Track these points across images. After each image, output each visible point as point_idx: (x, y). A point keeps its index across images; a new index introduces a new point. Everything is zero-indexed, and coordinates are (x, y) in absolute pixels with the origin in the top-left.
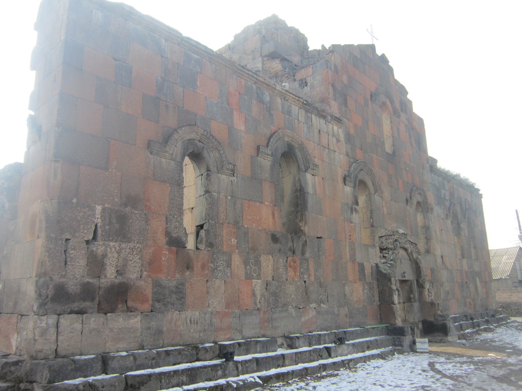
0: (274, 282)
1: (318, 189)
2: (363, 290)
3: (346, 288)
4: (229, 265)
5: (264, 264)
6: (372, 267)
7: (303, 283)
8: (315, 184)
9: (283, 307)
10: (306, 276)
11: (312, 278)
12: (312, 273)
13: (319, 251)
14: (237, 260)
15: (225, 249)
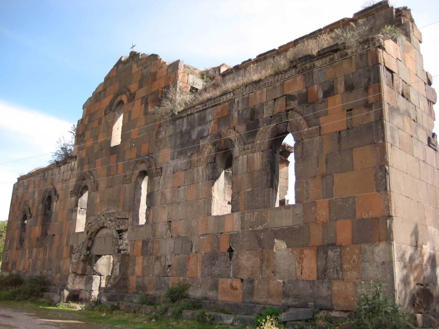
1: (57, 208)
11: (47, 257)
12: (47, 255)
14: (27, 251)
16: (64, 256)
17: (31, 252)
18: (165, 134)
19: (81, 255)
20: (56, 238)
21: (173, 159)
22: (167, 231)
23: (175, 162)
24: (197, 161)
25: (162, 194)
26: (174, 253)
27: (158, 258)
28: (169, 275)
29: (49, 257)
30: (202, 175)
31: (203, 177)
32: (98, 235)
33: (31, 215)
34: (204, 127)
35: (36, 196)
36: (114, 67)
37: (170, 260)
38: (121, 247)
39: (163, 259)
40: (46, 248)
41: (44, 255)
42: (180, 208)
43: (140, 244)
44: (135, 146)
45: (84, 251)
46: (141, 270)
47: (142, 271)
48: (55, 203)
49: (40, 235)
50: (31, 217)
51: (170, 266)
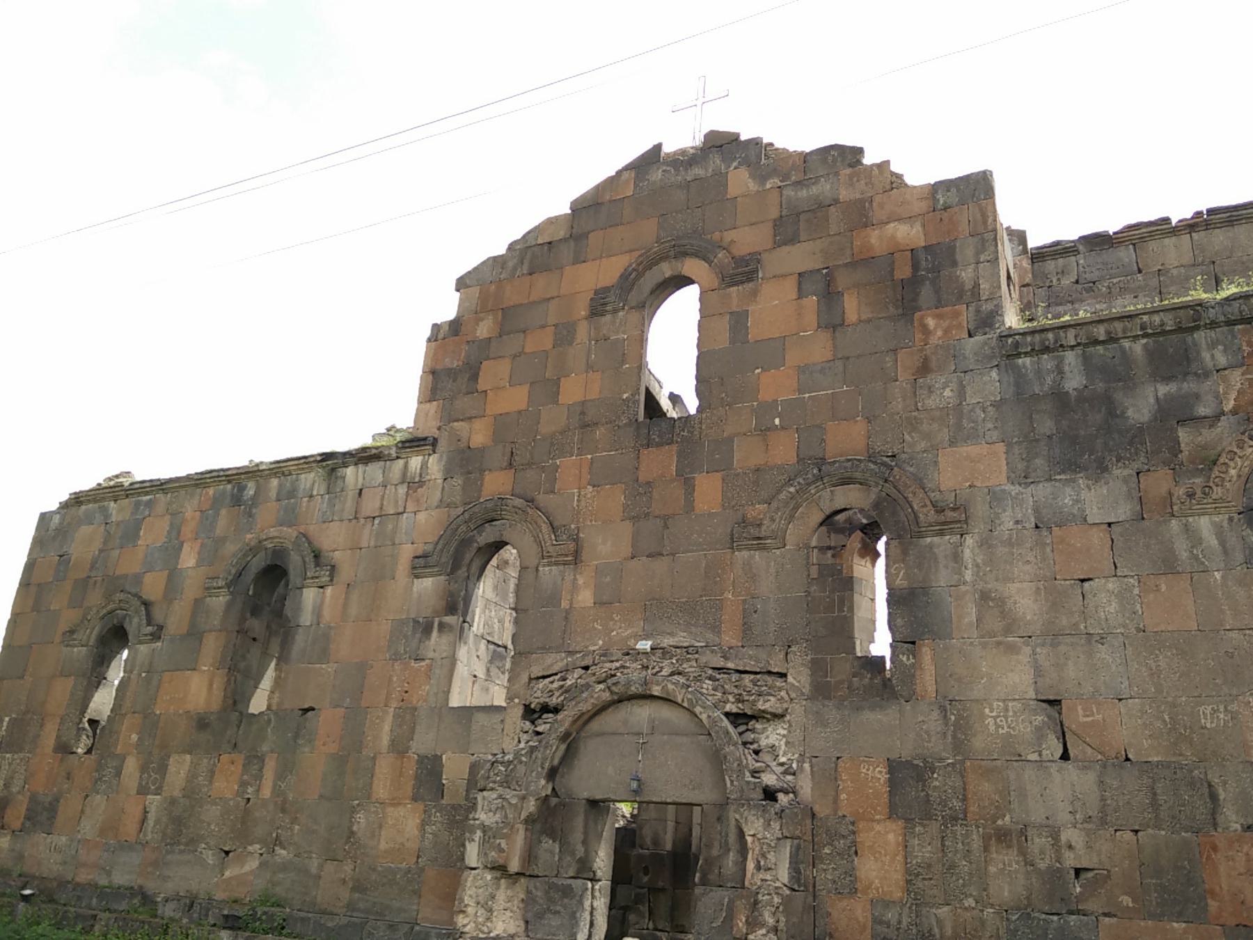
0: (182, 800)
2: (424, 824)
3: (361, 817)
4: (118, 773)
5: (172, 769)
6: (474, 768)
7: (243, 803)
8: (322, 602)
9: (187, 845)
10: (250, 790)
11: (266, 792)
13: (297, 736)
14: (131, 766)
15: (119, 750)
16: (381, 790)
17: (155, 768)
18: (961, 392)
19: (524, 798)
20: (328, 722)
21: (1025, 479)
22: (1039, 734)
23: (1042, 491)
24: (1191, 495)
25: (985, 596)
26: (1103, 822)
27: (1003, 836)
28: (1089, 906)
29: (277, 791)
30: (1223, 543)
31: (1225, 552)
32: (595, 725)
33: (161, 628)
34: (1189, 386)
35: (188, 559)
36: (619, 173)
37: (1078, 847)
38: (769, 779)
39: (1039, 842)
40: (255, 760)
41: (243, 784)
42: (1103, 652)
43: (880, 774)
44: (783, 428)
45: (542, 786)
46: (897, 876)
47: (908, 882)
48: (309, 596)
49: (216, 705)
50: (156, 636)
51: (1078, 872)
